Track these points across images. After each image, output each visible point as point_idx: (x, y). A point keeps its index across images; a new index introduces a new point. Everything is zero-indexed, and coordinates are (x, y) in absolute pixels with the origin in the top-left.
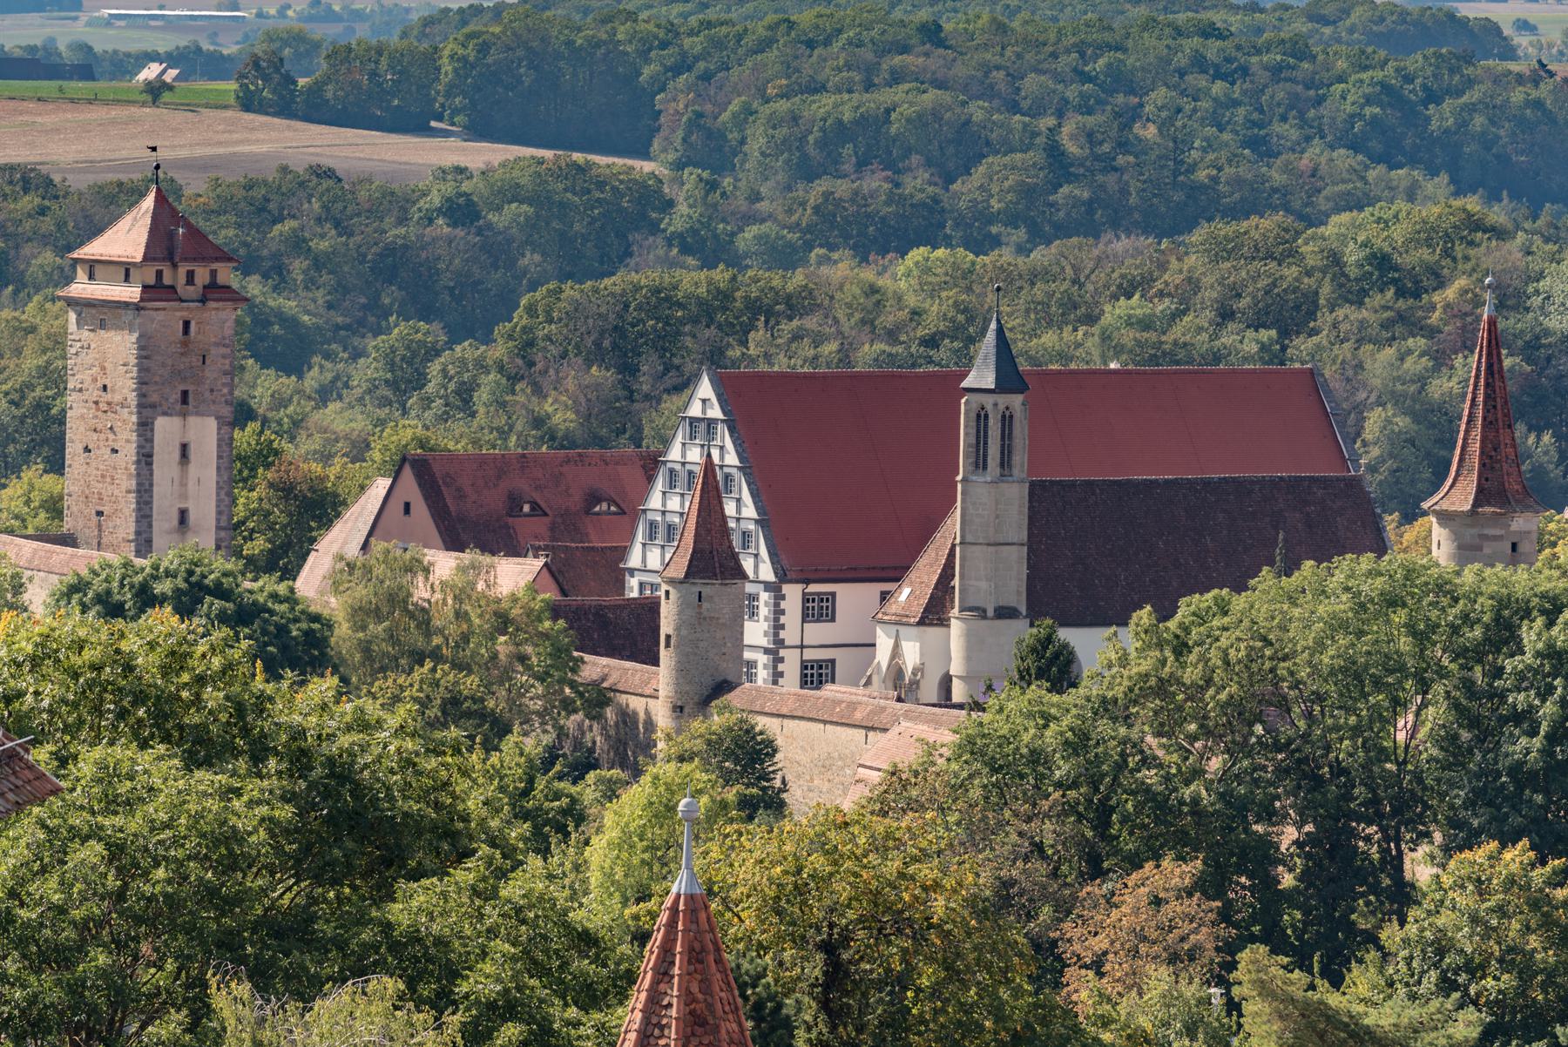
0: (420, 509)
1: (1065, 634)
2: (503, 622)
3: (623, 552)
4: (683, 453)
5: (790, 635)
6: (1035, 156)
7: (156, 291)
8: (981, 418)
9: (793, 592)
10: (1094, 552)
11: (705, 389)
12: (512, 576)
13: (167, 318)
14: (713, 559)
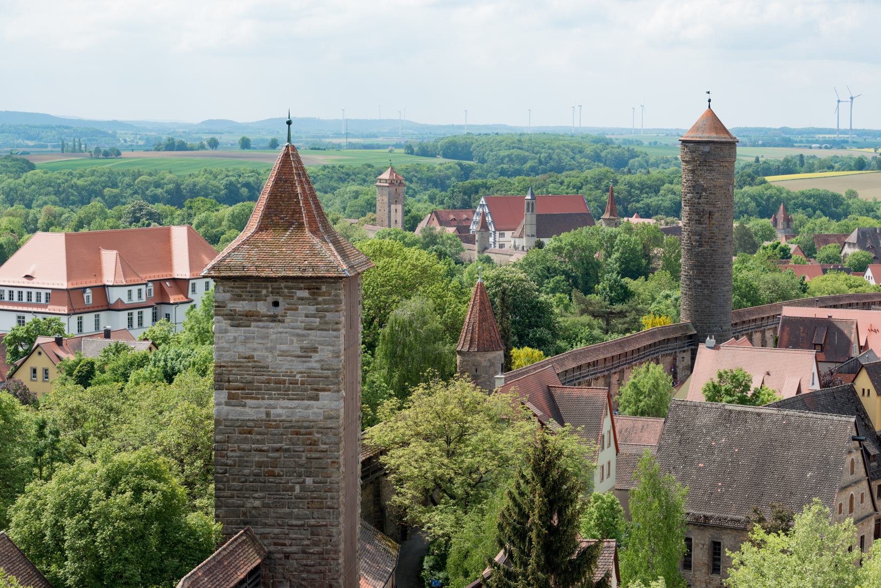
0: (435, 219)
1: (542, 240)
2: (449, 238)
4: (479, 210)
6: (536, 161)
7: (391, 183)
8: (528, 204)
9: (497, 233)
10: (547, 225)
11: (483, 199)
12: (451, 231)
13: (393, 189)
14: (484, 226)
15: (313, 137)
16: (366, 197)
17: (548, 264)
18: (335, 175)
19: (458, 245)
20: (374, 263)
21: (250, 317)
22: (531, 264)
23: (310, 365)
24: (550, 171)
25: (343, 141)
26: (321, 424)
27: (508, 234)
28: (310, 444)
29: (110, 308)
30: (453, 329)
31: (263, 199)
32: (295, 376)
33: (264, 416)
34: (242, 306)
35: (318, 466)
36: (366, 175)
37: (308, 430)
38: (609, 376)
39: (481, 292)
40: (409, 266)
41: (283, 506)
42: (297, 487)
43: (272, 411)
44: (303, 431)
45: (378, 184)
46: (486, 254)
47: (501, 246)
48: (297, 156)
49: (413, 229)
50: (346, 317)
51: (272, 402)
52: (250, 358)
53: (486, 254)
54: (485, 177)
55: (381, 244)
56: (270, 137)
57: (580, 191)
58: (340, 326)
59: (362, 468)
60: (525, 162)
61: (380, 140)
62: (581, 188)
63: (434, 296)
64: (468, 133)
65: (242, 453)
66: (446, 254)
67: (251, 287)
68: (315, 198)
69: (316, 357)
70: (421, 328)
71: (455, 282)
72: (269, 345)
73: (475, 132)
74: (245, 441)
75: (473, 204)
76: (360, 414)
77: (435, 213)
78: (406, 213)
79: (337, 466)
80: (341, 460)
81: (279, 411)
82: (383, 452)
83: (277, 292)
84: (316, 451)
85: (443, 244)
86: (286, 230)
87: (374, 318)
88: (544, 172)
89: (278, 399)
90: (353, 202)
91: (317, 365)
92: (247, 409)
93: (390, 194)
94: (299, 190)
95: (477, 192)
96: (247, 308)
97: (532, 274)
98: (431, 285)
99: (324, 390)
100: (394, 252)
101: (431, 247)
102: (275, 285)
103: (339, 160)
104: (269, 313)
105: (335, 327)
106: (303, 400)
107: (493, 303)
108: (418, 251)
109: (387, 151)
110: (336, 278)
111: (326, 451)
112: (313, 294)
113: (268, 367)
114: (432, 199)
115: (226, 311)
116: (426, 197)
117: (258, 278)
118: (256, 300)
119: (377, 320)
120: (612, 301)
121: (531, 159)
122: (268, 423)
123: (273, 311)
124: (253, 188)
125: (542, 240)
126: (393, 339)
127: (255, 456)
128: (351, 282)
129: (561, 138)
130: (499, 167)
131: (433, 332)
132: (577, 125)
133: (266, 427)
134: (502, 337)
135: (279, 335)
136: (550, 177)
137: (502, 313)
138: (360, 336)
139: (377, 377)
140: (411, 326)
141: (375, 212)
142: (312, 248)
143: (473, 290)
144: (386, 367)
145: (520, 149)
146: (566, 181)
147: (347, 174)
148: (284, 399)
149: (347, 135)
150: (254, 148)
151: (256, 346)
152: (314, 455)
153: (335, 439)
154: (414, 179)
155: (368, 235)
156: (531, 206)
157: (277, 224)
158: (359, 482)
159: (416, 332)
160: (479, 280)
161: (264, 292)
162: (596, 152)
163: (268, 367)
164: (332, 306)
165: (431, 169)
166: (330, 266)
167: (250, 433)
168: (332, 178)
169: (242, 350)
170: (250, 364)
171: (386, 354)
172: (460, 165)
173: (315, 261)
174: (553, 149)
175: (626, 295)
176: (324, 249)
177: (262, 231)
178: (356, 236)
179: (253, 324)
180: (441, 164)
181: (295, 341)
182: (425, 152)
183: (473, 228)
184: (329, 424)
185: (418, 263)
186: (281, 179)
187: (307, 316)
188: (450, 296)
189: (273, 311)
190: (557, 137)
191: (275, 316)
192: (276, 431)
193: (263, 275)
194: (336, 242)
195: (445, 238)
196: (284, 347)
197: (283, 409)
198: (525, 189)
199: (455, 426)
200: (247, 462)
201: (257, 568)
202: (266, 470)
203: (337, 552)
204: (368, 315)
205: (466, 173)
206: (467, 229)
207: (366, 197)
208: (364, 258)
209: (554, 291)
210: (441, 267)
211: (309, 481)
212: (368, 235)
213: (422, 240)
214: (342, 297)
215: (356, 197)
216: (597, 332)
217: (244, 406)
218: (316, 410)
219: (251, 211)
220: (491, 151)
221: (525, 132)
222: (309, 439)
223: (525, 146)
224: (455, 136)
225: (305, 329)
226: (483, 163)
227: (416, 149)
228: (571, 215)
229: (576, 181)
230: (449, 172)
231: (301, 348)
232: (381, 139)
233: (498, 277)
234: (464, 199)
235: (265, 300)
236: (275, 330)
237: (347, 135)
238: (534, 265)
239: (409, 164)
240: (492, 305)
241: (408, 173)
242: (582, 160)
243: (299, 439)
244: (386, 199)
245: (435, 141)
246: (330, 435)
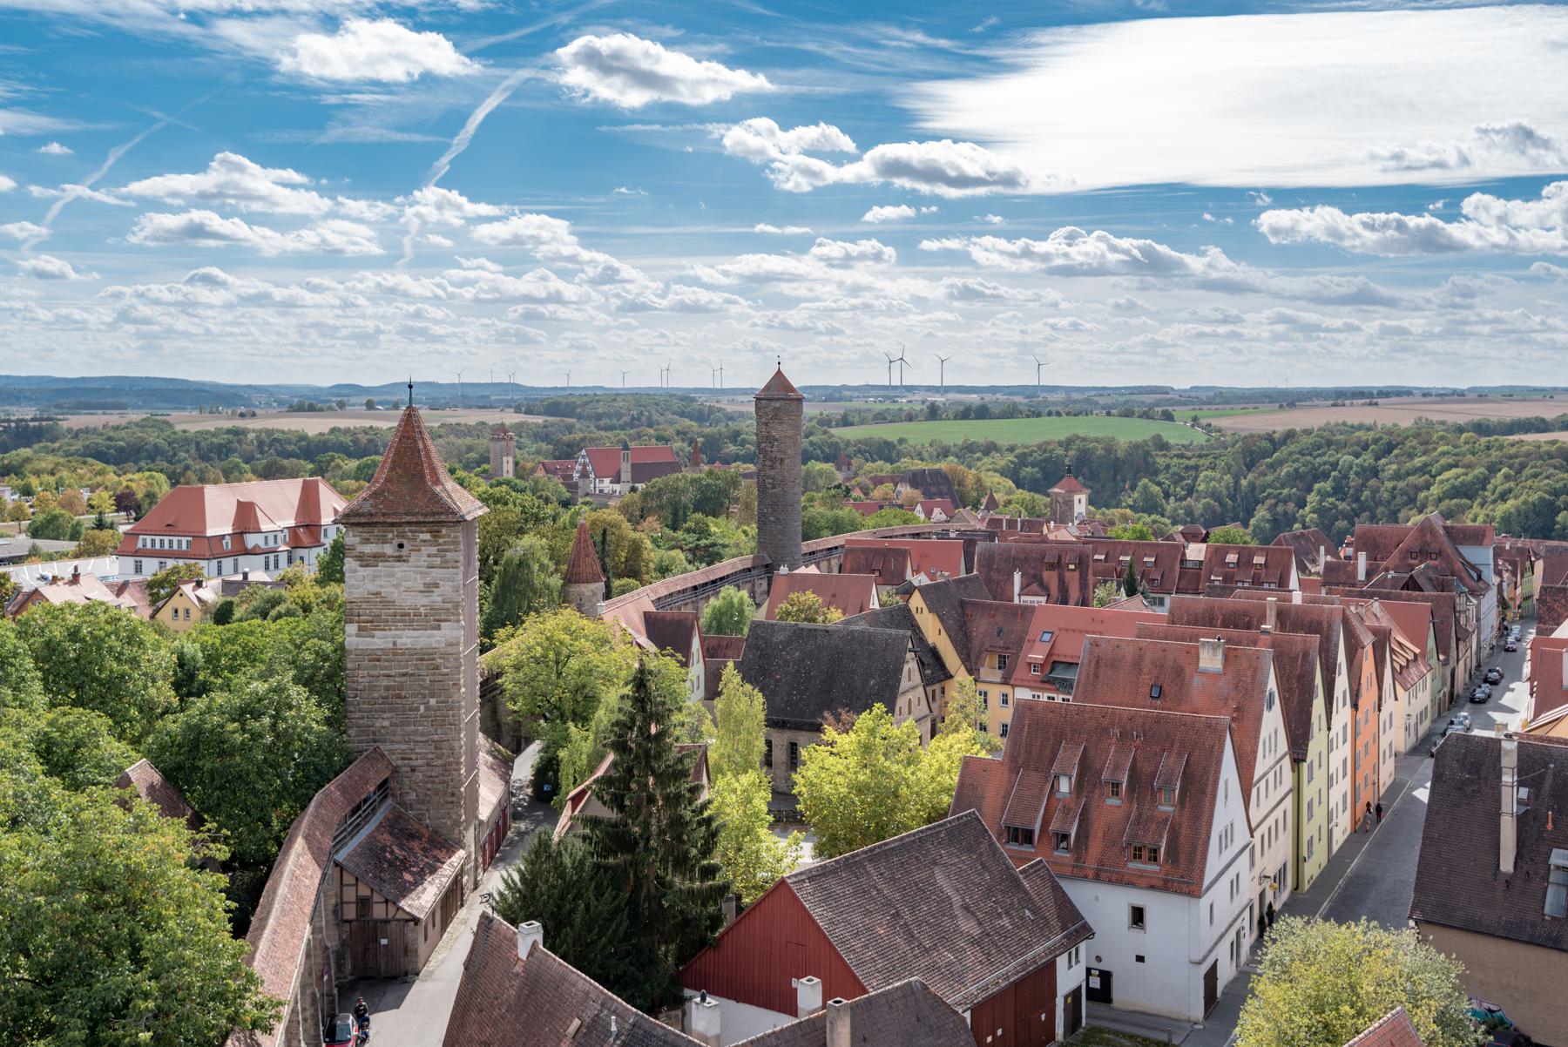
4: (581, 460)
14: (584, 475)
21: (378, 557)
29: (247, 553)
34: (369, 549)
35: (442, 687)
41: (409, 724)
42: (422, 708)
74: (375, 667)
81: (405, 640)
115: (355, 553)
122: (395, 652)
158: (478, 700)
169: (372, 587)
183: (576, 475)
184: (450, 650)
196: (408, 584)
197: (409, 638)
201: (385, 782)
203: (459, 763)
206: (571, 477)
211: (433, 701)
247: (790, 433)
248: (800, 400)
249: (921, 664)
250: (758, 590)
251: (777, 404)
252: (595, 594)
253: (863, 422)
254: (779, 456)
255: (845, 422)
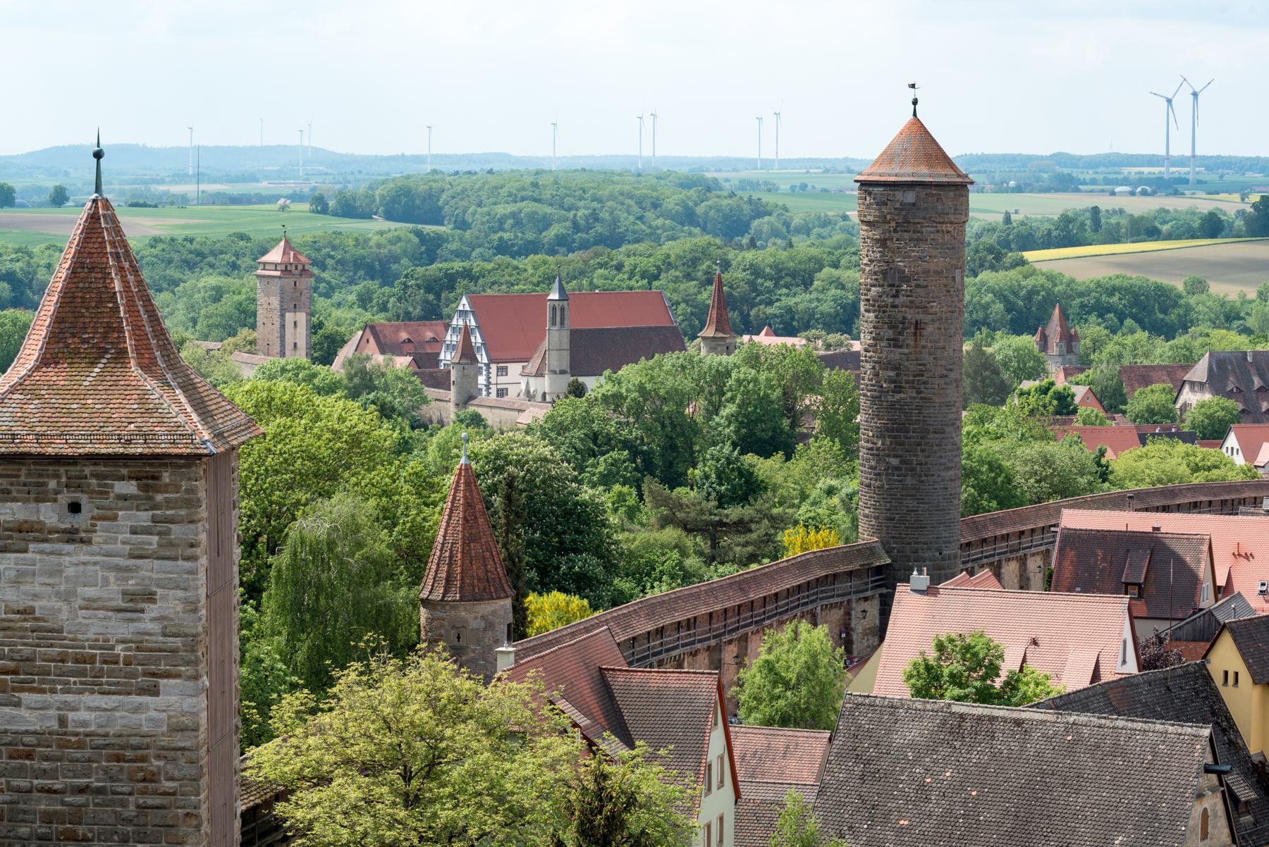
0: (372, 340)
1: (581, 379)
2: (398, 378)
3: (438, 354)
4: (457, 322)
5: (493, 380)
6: (568, 224)
7: (286, 271)
8: (554, 309)
9: (494, 367)
10: (591, 350)
11: (464, 301)
13: (289, 282)
14: (468, 353)
15: (134, 182)
16: (236, 298)
17: (595, 427)
18: (176, 257)
19: (417, 392)
20: (263, 429)
22: (561, 429)
23: (141, 626)
24: (596, 244)
25: (190, 189)
26: (164, 741)
27: (515, 369)
28: (144, 780)
30: (414, 556)
31: (49, 305)
32: (112, 648)
33: (55, 725)
36: (237, 255)
37: (140, 752)
38: (718, 649)
39: (467, 484)
40: (328, 435)
43: (71, 715)
44: (129, 754)
45: (260, 272)
46: (471, 409)
47: (502, 393)
48: (113, 220)
49: (327, 359)
50: (209, 533)
51: (70, 698)
52: (27, 612)
53: (471, 409)
54: (466, 256)
55: (270, 390)
56: (51, 184)
57: (656, 283)
58: (198, 551)
59: (243, 826)
60: (546, 228)
61: (263, 187)
62: (656, 277)
63: (374, 491)
64: (434, 172)
65: (16, 796)
66: (393, 410)
67: (29, 475)
68: (148, 301)
69: (153, 610)
70: (352, 554)
71: (413, 464)
72: (63, 588)
73: (449, 168)
74: (21, 772)
75: (445, 311)
76: (237, 721)
77: (371, 328)
78: (315, 328)
79: (195, 823)
80: (204, 812)
81: (83, 715)
82: (282, 796)
83: (76, 484)
84: (155, 793)
85: (386, 389)
86: (93, 364)
87: (259, 534)
88: (584, 246)
89: (81, 692)
90: (212, 308)
91: (155, 627)
92: (23, 712)
93: (282, 292)
94: (117, 285)
95: (452, 288)
96: (21, 516)
97: (563, 448)
98: (369, 470)
99: (168, 675)
100: (295, 406)
101: (363, 397)
102: (74, 470)
103: (184, 227)
104: (63, 526)
105: (189, 552)
106: (129, 694)
107: (489, 505)
108: (341, 403)
109: (275, 207)
110: (189, 456)
111: (174, 794)
112: (145, 488)
113: (60, 631)
114: (364, 301)
116: (352, 298)
117: (41, 458)
118: (37, 500)
119: (264, 538)
120: (722, 501)
121: (559, 221)
122: (63, 738)
123: (70, 521)
124: (20, 281)
125: (581, 379)
126: (297, 579)
127: (39, 801)
128: (218, 464)
129: (616, 178)
130: (496, 237)
131: (374, 562)
132: (647, 152)
133: (60, 747)
134: (509, 571)
135: (81, 568)
136: (597, 255)
137: (508, 524)
138: (236, 569)
139: (267, 650)
140: (331, 550)
141: (253, 327)
142: (143, 398)
143: (450, 480)
144: (285, 633)
145: (535, 200)
146: (628, 263)
147: (199, 254)
148: (93, 692)
149: (199, 178)
150: (22, 206)
151: (37, 589)
152: (151, 801)
153: (190, 771)
154: (330, 262)
155: (244, 373)
156: (559, 315)
157: (76, 353)
159: (342, 563)
160: (463, 461)
161: (52, 484)
162: (686, 207)
163: (60, 631)
164: (183, 512)
165: (361, 242)
166: (178, 433)
167: (29, 756)
168: (170, 262)
170: (28, 625)
171: (282, 607)
172: (418, 234)
173: (149, 424)
174: (600, 201)
175: (749, 488)
176: (166, 400)
177: (47, 365)
178: (218, 375)
179: (32, 546)
180: (381, 233)
181: (112, 579)
182: (350, 209)
183: (446, 357)
184: (180, 741)
185: (343, 427)
186: (82, 265)
187: (134, 531)
188: (406, 492)
189: (70, 521)
190: (608, 177)
191: (76, 531)
192: (78, 754)
193: (50, 450)
194: (189, 388)
195: (390, 376)
196: (90, 592)
197: (91, 711)
198: (548, 280)
199: (420, 746)
200: (25, 812)
202: (61, 827)
204: (248, 529)
205: (430, 249)
206: (434, 360)
207: (236, 298)
208: (240, 418)
209: (606, 480)
210: (387, 433)
212: (244, 373)
213: (345, 382)
214: (202, 494)
215: (217, 299)
216: (692, 562)
217: (18, 704)
218: (153, 714)
219: (26, 326)
220: (480, 205)
221: (546, 168)
222: (141, 769)
223: (547, 194)
224: (408, 177)
225: (132, 556)
226: (465, 230)
227: (332, 204)
228: (637, 330)
229: (647, 264)
230: (397, 249)
231: (125, 593)
232: (265, 184)
233: (497, 454)
234: (427, 302)
235: (55, 500)
236: (75, 559)
237: (199, 178)
238: (567, 429)
239: (320, 233)
240: (488, 509)
241: (318, 250)
242: (660, 222)
243: (122, 769)
244: (275, 302)
245: (370, 188)
246: (182, 762)
247: (938, 263)
248: (960, 188)
249: (1231, 799)
250: (859, 626)
251: (910, 197)
252: (489, 626)
253: (1114, 237)
254: (910, 315)
255: (1067, 233)
